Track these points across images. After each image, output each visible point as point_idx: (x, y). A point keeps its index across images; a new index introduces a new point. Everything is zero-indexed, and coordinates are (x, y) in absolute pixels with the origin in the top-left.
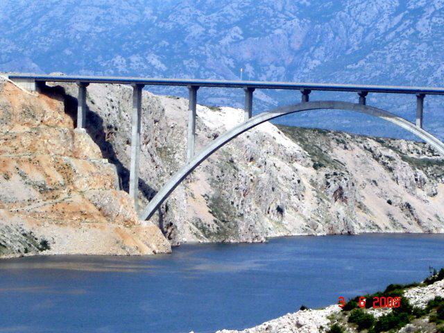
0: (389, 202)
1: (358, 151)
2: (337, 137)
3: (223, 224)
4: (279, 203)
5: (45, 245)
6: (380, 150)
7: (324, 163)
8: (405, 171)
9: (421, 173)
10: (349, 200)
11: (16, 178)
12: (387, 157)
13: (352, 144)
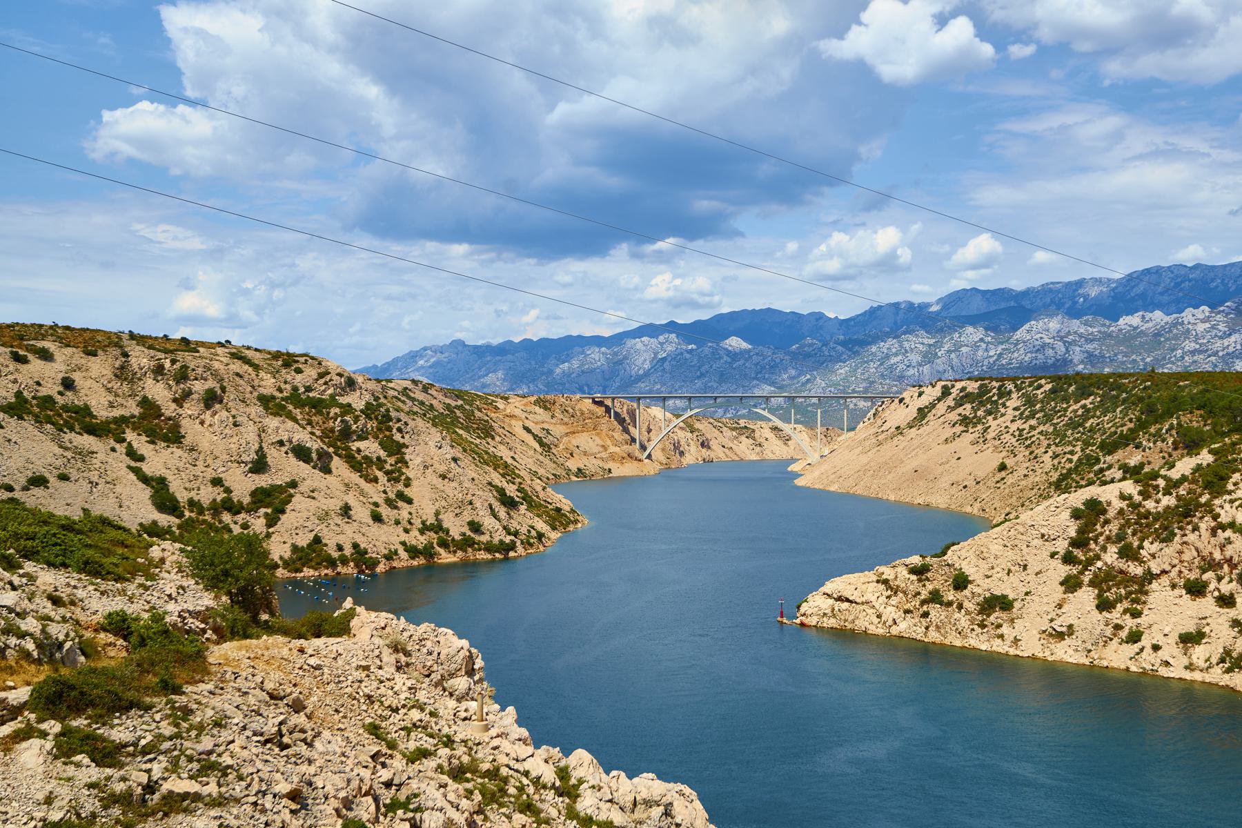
0: (724, 447)
1: (706, 424)
6: (715, 423)
8: (727, 433)
9: (734, 433)
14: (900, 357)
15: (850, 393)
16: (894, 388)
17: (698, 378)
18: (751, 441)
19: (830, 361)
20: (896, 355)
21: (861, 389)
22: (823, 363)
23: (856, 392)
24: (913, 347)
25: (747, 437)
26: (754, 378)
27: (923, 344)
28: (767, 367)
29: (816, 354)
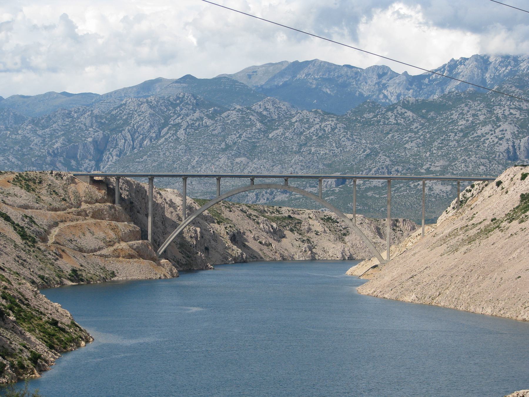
1: (238, 213)
2: (225, 205)
3: (188, 259)
4: (206, 245)
5: (113, 274)
7: (221, 220)
10: (239, 242)
11: (88, 234)
12: (255, 215)
13: (233, 208)
14: (489, 127)
15: (422, 173)
16: (482, 167)
17: (224, 150)
18: (296, 235)
19: (397, 131)
20: (484, 123)
21: (438, 169)
22: (388, 133)
23: (432, 172)
24: (507, 113)
25: (292, 230)
26: (296, 153)
27: (520, 109)
28: (314, 137)
29: (379, 121)
